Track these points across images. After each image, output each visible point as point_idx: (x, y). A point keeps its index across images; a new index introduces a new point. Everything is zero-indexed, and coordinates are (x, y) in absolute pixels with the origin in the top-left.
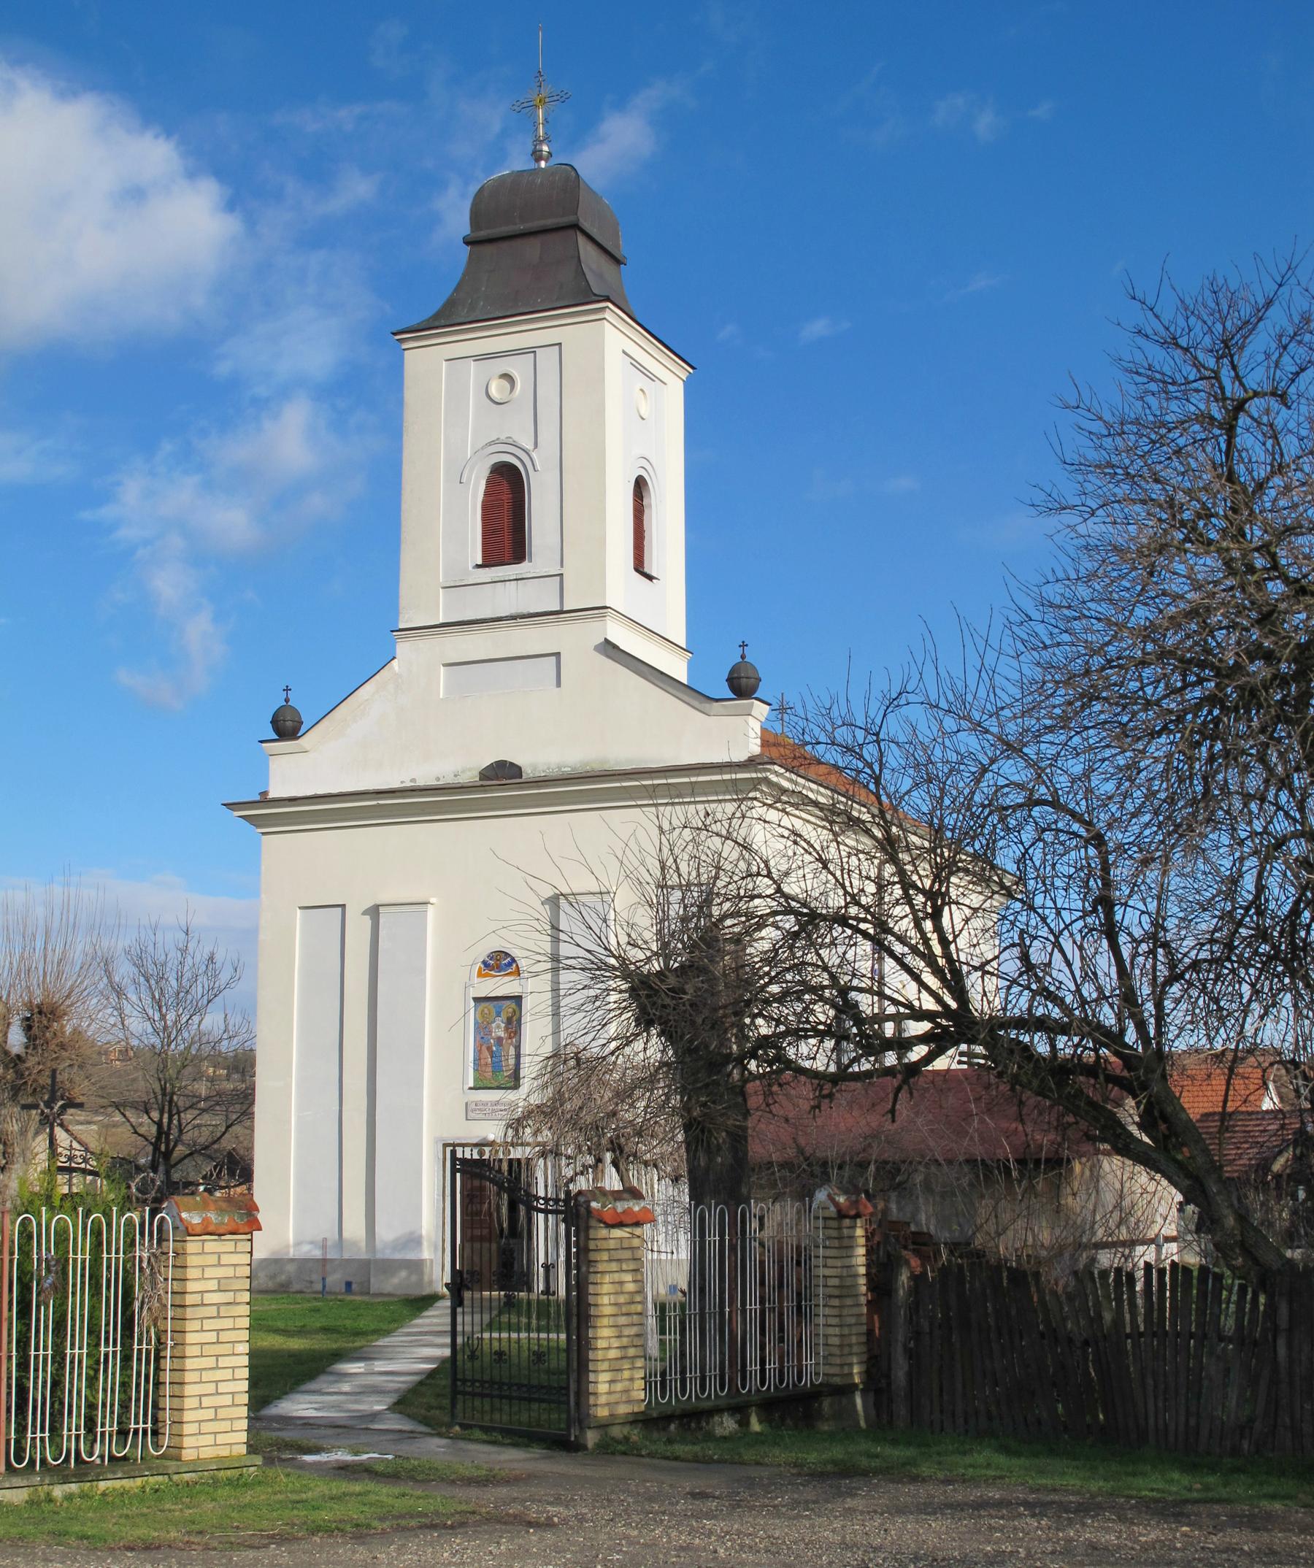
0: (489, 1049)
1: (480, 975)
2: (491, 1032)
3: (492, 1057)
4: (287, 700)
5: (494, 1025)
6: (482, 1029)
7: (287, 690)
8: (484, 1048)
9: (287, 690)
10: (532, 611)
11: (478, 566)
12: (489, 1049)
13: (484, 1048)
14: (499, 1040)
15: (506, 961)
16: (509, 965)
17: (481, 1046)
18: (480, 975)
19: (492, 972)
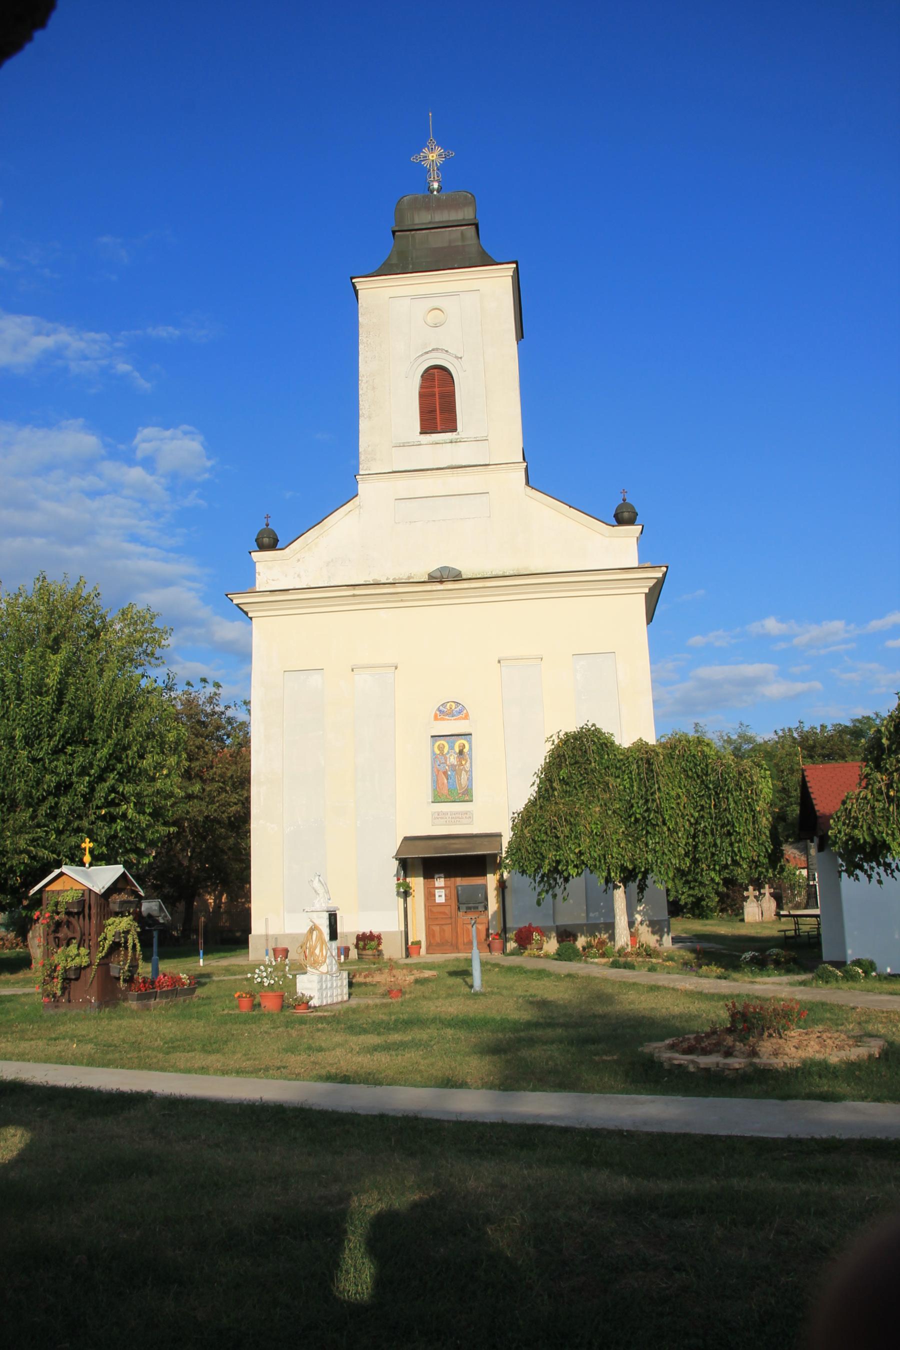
0: (445, 773)
1: (436, 718)
2: (446, 760)
3: (447, 779)
4: (267, 525)
5: (448, 756)
6: (437, 759)
7: (267, 517)
8: (441, 773)
9: (267, 517)
10: (464, 464)
11: (421, 433)
12: (445, 773)
13: (441, 773)
14: (453, 767)
15: (457, 709)
16: (460, 712)
17: (438, 771)
18: (436, 718)
19: (447, 717)
